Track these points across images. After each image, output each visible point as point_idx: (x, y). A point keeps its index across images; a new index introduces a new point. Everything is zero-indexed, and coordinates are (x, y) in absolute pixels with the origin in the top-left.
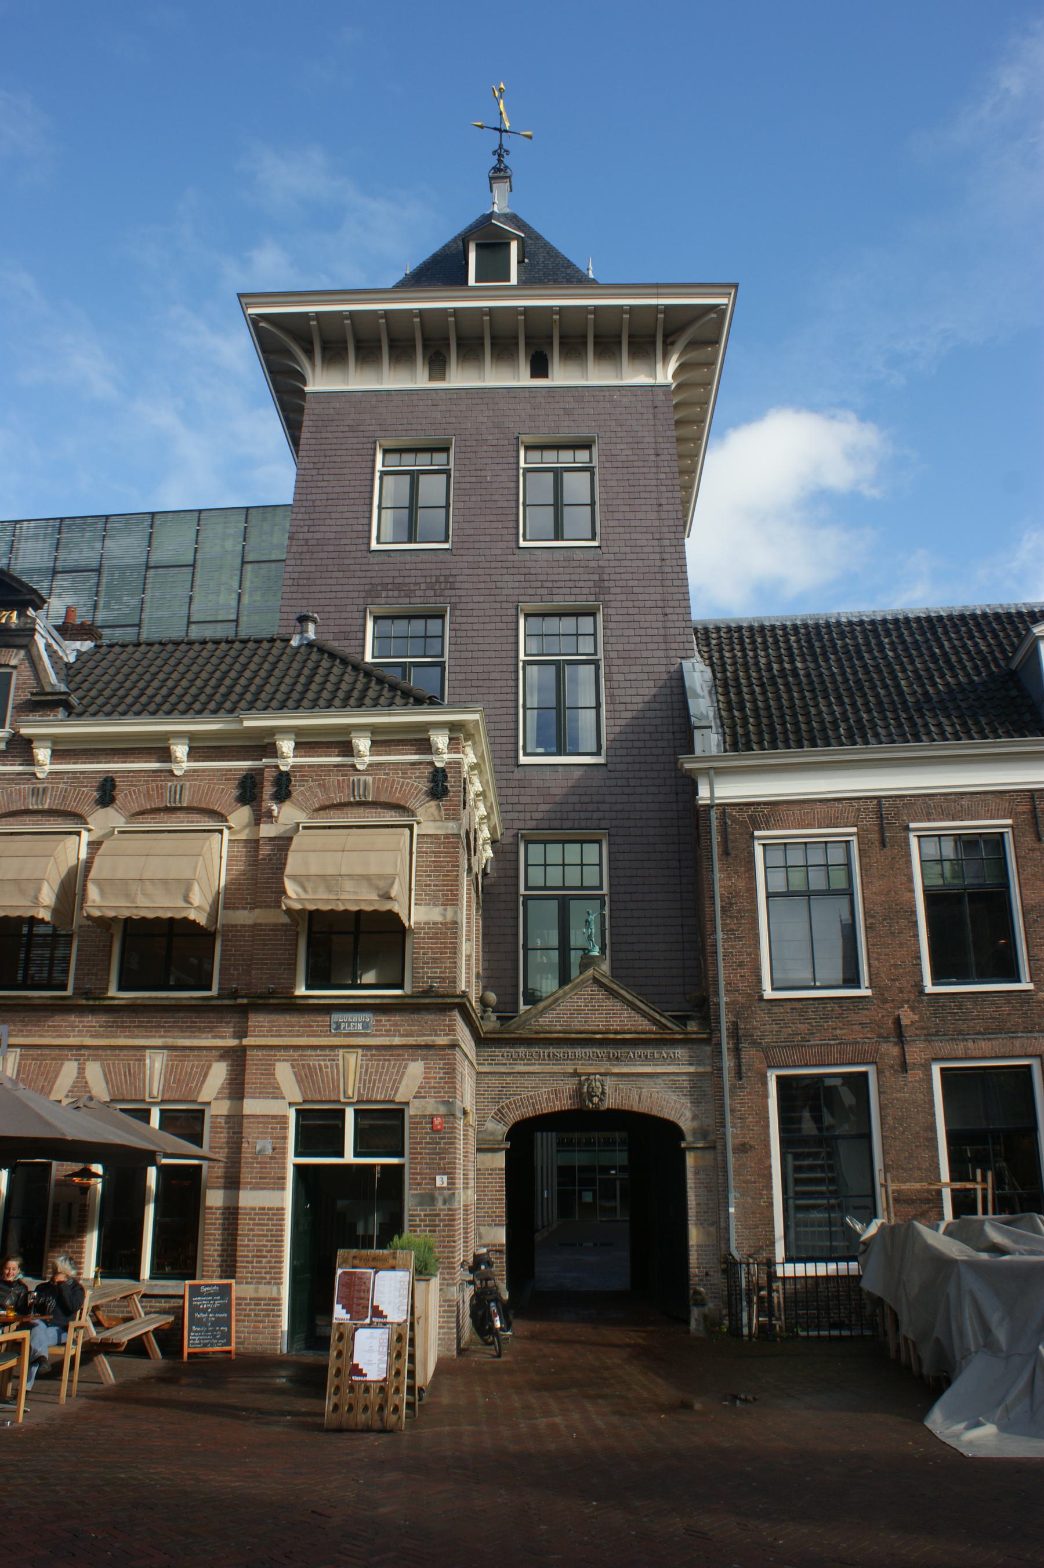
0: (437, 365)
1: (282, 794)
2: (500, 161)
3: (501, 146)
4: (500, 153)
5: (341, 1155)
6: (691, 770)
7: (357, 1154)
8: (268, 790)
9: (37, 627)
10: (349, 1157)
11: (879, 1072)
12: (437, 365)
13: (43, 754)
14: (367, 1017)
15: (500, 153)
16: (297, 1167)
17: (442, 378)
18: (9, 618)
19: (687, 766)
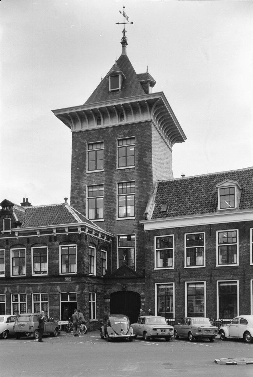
0: (99, 121)
1: (55, 240)
2: (124, 35)
3: (124, 29)
4: (124, 32)
5: (67, 300)
6: (142, 223)
7: (70, 300)
8: (53, 239)
9: (13, 210)
10: (69, 301)
11: (175, 284)
12: (99, 121)
13: (16, 234)
14: (70, 278)
15: (124, 32)
16: (61, 302)
17: (100, 124)
18: (8, 209)
19: (141, 223)
